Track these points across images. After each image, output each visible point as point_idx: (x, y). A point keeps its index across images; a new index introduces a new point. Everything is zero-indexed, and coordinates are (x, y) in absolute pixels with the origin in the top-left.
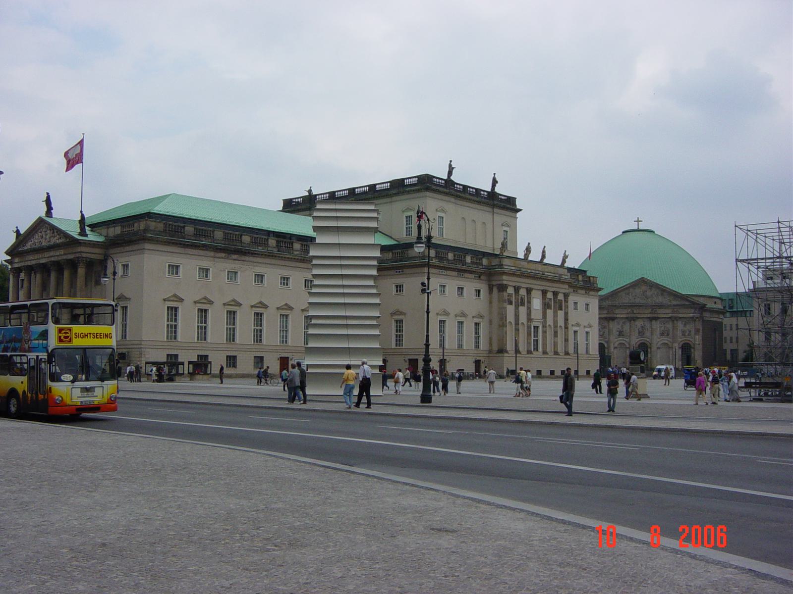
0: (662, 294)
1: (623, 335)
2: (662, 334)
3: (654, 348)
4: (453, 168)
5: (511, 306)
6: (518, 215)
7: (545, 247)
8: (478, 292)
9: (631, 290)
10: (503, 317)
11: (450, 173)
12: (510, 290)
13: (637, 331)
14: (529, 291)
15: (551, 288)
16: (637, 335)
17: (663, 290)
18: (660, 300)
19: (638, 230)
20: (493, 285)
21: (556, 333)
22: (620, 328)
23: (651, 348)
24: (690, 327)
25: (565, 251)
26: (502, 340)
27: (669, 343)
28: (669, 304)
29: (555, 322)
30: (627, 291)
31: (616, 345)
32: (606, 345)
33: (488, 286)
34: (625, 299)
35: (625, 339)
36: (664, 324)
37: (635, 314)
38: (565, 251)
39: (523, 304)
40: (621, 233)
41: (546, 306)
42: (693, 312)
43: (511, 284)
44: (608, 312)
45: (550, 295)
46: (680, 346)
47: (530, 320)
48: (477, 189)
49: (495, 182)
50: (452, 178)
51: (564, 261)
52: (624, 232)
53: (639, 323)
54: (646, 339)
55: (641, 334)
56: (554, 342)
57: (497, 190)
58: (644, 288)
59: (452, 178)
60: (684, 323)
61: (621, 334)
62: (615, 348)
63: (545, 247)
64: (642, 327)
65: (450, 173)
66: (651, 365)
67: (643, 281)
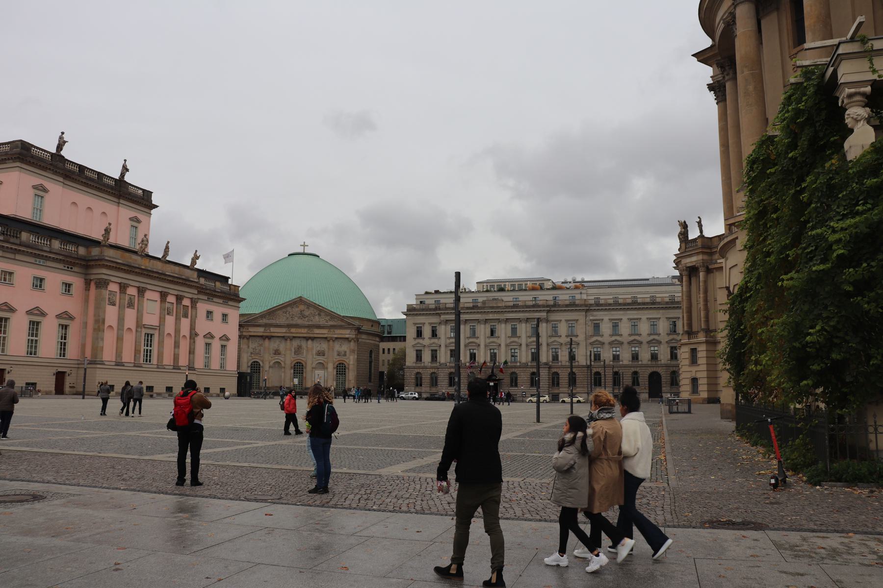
0: (319, 315)
3: (309, 368)
4: (65, 142)
5: (111, 307)
6: (153, 211)
7: (168, 242)
8: (68, 286)
9: (289, 309)
10: (100, 322)
11: (60, 147)
12: (113, 287)
14: (141, 291)
15: (173, 290)
16: (293, 354)
17: (320, 310)
18: (317, 320)
19: (304, 254)
20: (91, 280)
21: (177, 345)
23: (306, 368)
24: (345, 347)
25: (196, 251)
26: (97, 350)
27: (324, 363)
28: (326, 323)
29: (177, 331)
30: (284, 310)
31: (272, 363)
33: (83, 280)
34: (282, 319)
38: (196, 251)
39: (131, 305)
40: (287, 256)
41: (165, 312)
43: (113, 279)
45: (171, 299)
46: (335, 366)
47: (139, 325)
48: (99, 174)
49: (125, 169)
50: (63, 153)
51: (194, 261)
52: (289, 255)
55: (297, 353)
56: (174, 354)
57: (127, 178)
58: (302, 307)
59: (63, 153)
63: (168, 242)
65: (60, 147)
66: (305, 385)
67: (300, 301)
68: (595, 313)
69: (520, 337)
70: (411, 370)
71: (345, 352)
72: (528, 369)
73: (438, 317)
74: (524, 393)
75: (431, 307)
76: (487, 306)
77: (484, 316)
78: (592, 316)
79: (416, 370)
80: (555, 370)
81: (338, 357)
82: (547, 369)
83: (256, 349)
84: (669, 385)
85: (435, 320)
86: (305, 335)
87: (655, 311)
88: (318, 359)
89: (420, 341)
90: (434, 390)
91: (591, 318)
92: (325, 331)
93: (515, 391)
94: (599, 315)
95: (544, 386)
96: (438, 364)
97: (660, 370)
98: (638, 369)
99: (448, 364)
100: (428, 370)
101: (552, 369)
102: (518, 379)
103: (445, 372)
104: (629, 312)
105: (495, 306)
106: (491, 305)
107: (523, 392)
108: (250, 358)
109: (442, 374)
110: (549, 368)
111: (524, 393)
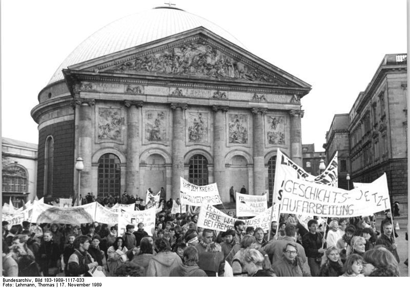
1: (159, 139)
2: (234, 140)
13: (187, 131)
16: (187, 139)
22: (154, 126)
23: (213, 165)
27: (247, 157)
32: (123, 159)
35: (162, 147)
36: (237, 121)
37: (184, 97)
42: (289, 101)
44: (128, 89)
46: (267, 162)
53: (190, 117)
54: (205, 148)
60: (272, 121)
61: (154, 136)
62: (143, 164)
64: (197, 124)
71: (282, 136)
81: (271, 145)
83: (110, 130)
86: (212, 103)
88: (236, 148)
92: (247, 96)
108: (98, 147)
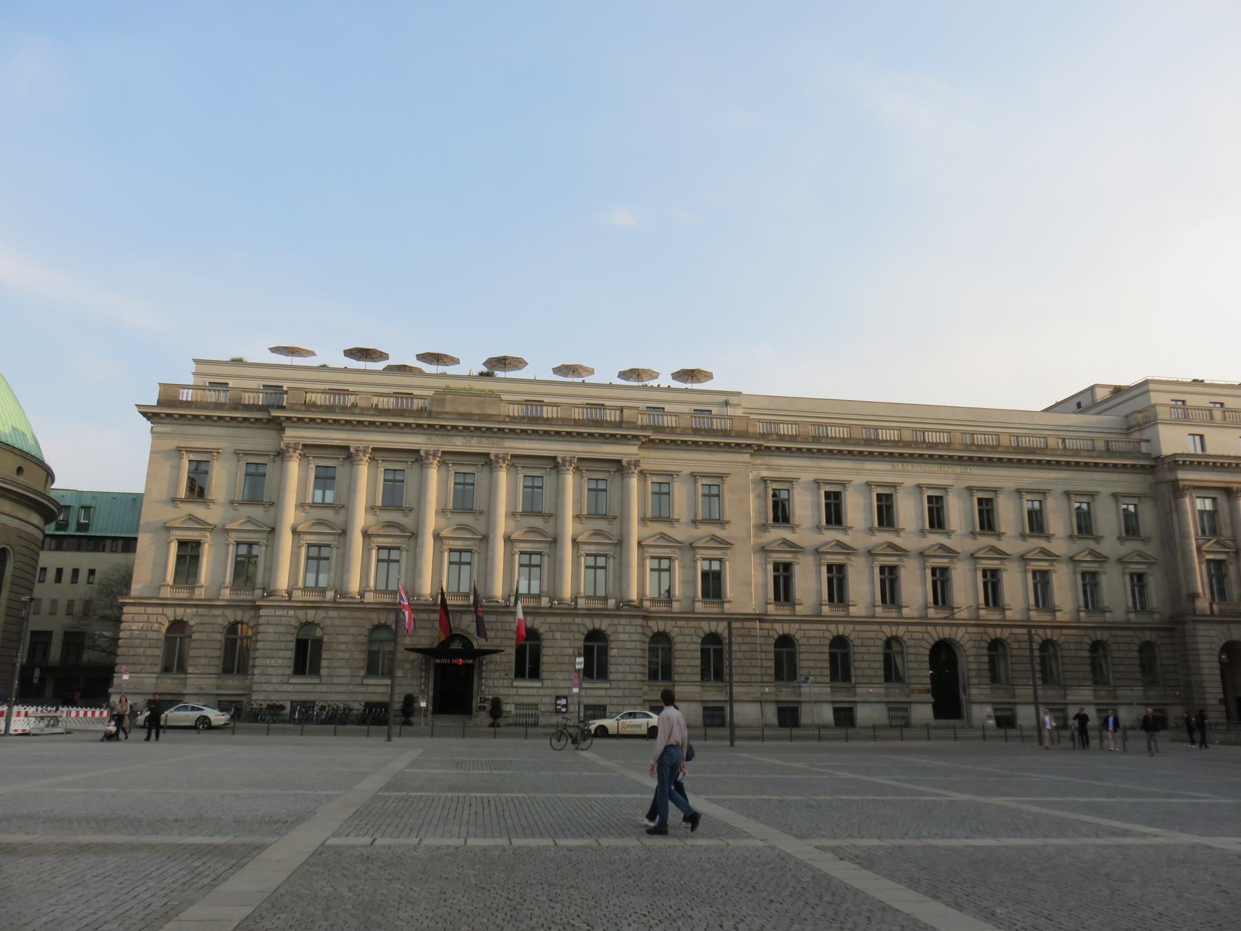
68: (776, 461)
69: (551, 515)
70: (149, 610)
72: (578, 620)
73: (273, 434)
74: (563, 702)
75: (248, 399)
76: (448, 408)
77: (436, 440)
78: (769, 467)
79: (170, 612)
80: (660, 626)
82: (640, 621)
84: (988, 681)
85: (259, 440)
87: (935, 468)
89: (198, 510)
90: (233, 685)
91: (765, 474)
93: (534, 691)
94: (785, 467)
95: (630, 677)
96: (258, 593)
97: (960, 635)
98: (901, 631)
99: (297, 595)
100: (218, 612)
101: (652, 623)
102: (544, 651)
103: (285, 621)
104: (869, 465)
105: (476, 411)
106: (462, 409)
107: (558, 698)
109: (270, 629)
110: (645, 618)
111: (563, 702)
